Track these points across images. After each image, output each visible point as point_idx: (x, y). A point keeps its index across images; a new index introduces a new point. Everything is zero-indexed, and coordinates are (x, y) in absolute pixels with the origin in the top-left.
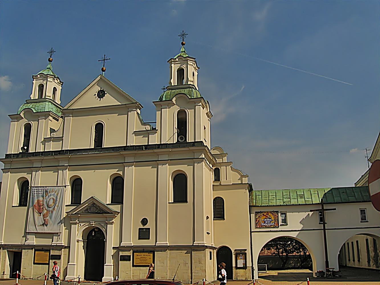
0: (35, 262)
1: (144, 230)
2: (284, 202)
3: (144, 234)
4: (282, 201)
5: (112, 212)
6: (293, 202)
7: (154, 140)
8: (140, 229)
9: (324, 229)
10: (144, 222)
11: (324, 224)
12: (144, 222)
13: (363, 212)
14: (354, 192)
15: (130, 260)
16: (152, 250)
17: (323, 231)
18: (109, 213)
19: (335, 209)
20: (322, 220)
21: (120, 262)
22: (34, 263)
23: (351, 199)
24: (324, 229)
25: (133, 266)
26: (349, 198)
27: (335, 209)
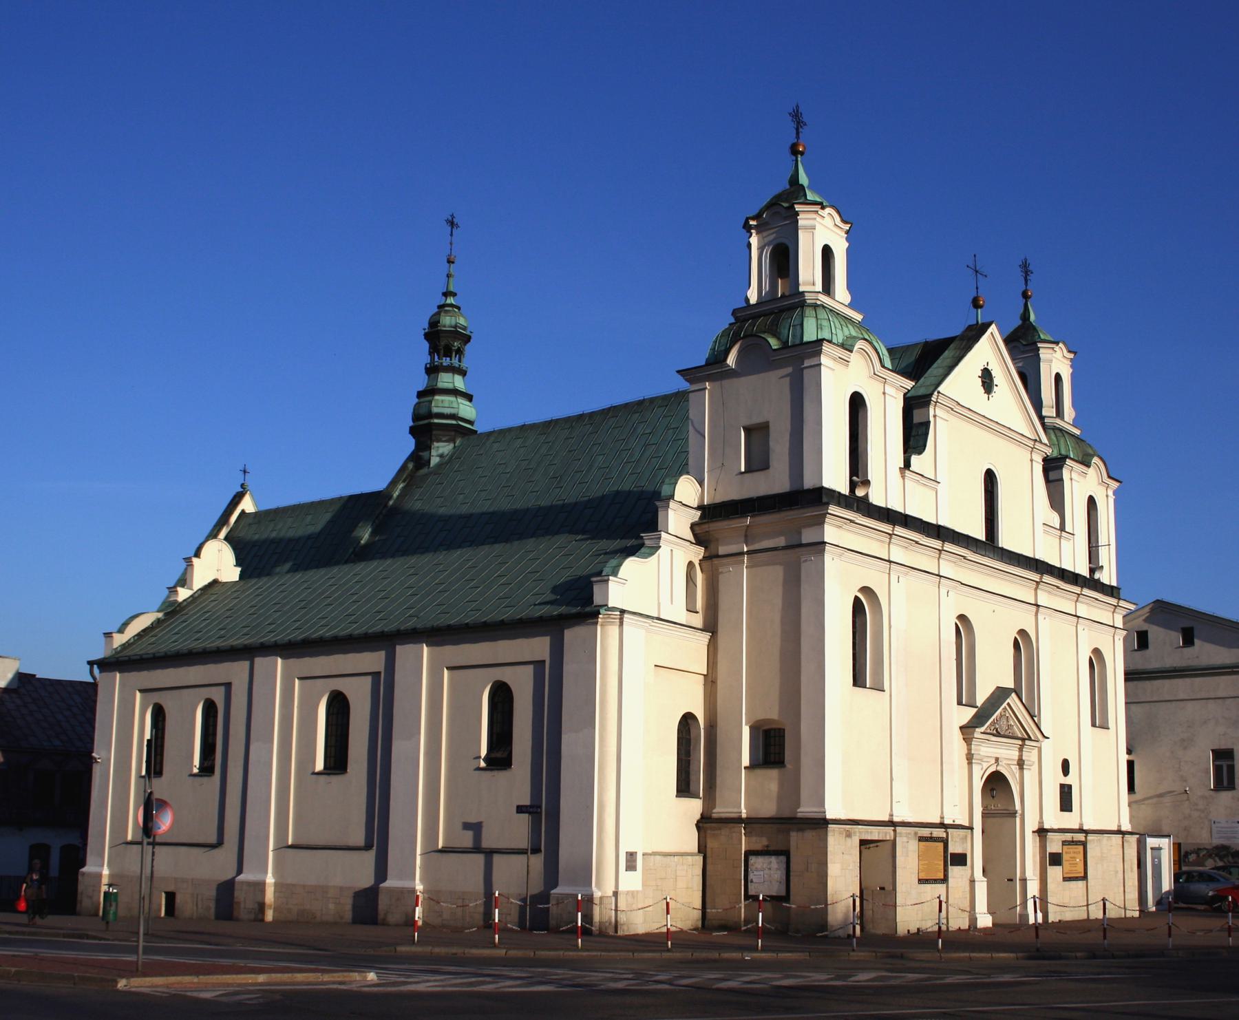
8: (1062, 786)
16: (1080, 838)
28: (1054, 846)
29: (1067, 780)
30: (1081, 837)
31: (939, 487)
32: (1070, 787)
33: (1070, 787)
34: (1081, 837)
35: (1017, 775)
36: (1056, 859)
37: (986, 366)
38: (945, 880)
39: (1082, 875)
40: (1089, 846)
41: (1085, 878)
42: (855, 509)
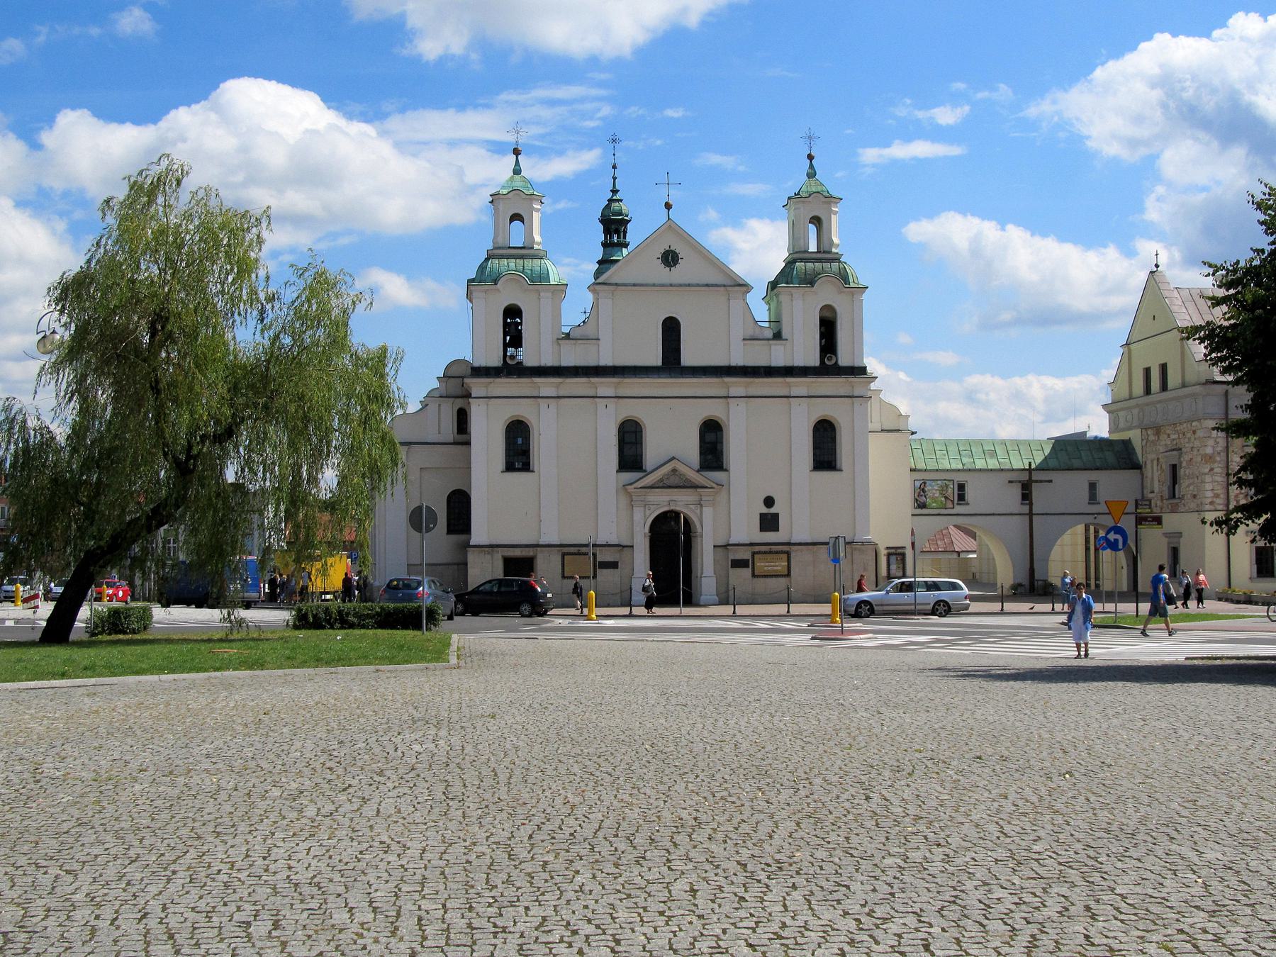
0: (566, 575)
1: (770, 516)
2: (963, 465)
3: (769, 522)
4: (959, 461)
5: (714, 485)
6: (980, 464)
7: (778, 356)
8: (762, 515)
9: (1031, 514)
10: (769, 502)
11: (1031, 504)
12: (769, 502)
13: (1092, 486)
14: (1079, 451)
15: (748, 567)
16: (785, 550)
17: (1028, 517)
18: (706, 487)
19: (1050, 481)
20: (1026, 496)
21: (730, 569)
22: (563, 577)
23: (1076, 463)
24: (1031, 514)
25: (754, 575)
26: (1073, 461)
27: (1050, 481)
28: (744, 554)
29: (773, 510)
30: (785, 548)
31: (600, 342)
32: (776, 516)
33: (776, 516)
34: (785, 548)
35: (698, 511)
36: (737, 564)
37: (668, 249)
38: (595, 577)
39: (786, 573)
40: (793, 555)
41: (789, 575)
42: (505, 373)
